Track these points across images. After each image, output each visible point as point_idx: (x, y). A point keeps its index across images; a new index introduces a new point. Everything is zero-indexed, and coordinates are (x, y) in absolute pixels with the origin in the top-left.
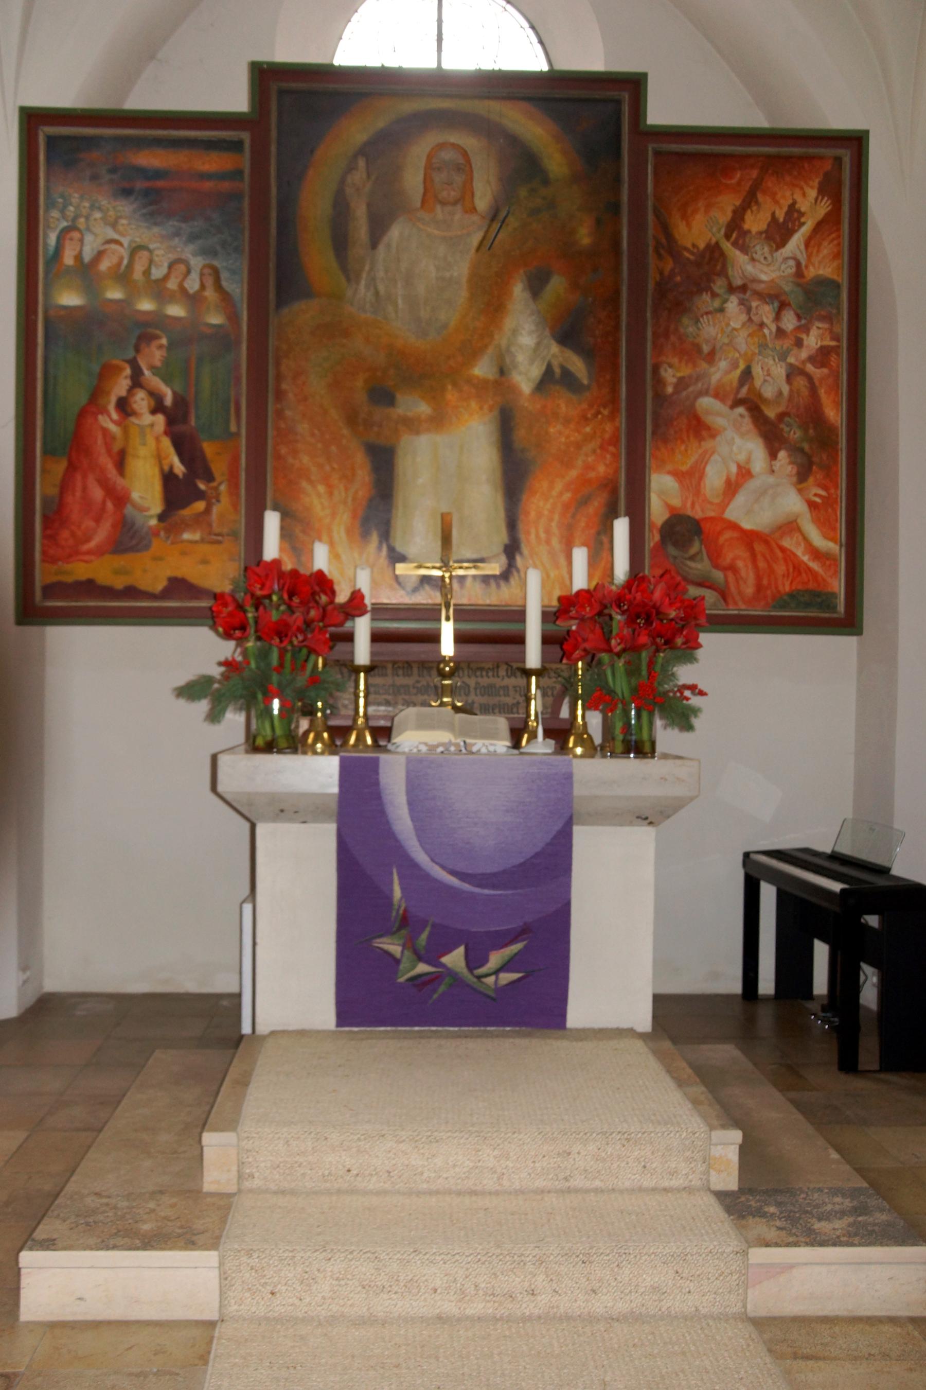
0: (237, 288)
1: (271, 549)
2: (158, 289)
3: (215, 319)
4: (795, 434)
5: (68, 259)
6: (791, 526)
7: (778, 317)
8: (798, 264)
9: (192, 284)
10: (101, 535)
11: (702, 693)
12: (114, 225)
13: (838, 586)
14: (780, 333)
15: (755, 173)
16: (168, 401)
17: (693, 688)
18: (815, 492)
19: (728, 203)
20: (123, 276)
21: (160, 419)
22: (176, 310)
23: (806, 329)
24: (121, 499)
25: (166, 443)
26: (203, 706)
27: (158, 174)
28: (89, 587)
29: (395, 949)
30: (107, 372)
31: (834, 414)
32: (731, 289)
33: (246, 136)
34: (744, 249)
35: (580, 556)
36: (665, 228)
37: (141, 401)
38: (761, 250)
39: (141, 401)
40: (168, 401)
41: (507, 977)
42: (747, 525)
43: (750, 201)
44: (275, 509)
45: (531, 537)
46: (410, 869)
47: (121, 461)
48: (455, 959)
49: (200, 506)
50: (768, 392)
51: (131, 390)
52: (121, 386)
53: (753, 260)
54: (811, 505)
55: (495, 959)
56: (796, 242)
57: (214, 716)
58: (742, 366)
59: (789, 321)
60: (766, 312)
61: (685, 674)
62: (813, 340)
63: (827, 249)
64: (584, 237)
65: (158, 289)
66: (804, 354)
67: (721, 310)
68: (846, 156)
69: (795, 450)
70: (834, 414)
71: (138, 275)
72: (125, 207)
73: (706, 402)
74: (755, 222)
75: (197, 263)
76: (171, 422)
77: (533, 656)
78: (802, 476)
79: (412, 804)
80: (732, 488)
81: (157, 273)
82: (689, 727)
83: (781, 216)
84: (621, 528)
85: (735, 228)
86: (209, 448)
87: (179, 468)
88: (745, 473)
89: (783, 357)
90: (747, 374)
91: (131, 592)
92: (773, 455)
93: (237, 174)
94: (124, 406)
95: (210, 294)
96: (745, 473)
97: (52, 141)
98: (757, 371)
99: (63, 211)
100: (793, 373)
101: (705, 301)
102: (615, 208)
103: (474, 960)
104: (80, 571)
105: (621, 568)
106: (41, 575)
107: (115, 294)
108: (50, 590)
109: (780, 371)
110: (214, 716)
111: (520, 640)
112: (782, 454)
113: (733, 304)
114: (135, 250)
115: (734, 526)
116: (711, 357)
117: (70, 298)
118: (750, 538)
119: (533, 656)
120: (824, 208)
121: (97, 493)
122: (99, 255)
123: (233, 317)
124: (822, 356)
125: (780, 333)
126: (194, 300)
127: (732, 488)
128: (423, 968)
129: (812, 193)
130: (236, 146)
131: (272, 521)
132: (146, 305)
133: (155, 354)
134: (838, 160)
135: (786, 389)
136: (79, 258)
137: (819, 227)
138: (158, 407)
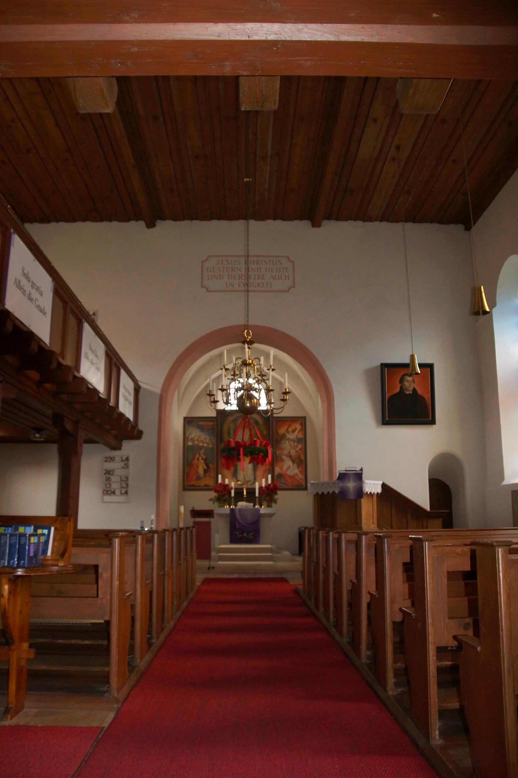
0: (215, 442)
1: (220, 481)
2: (202, 442)
3: (211, 446)
4: (297, 461)
5: (190, 438)
6: (296, 475)
7: (294, 443)
8: (297, 436)
9: (208, 441)
10: (195, 478)
11: (278, 499)
12: (196, 433)
13: (304, 483)
14: (294, 446)
15: (289, 423)
16: (204, 458)
17: (277, 498)
18: (300, 469)
19: (286, 427)
20: (198, 440)
21: (203, 461)
22: (205, 445)
23: (298, 445)
24: (197, 472)
25: (204, 465)
26: (212, 502)
27: (202, 425)
28: (193, 485)
29: (237, 533)
30: (195, 454)
31: (303, 457)
32: (287, 439)
33: (215, 420)
34: (288, 434)
35: (264, 480)
36: (277, 431)
37: (200, 458)
38: (291, 434)
39: (200, 458)
40: (204, 458)
41: (252, 537)
42: (289, 474)
43: (289, 426)
44: (220, 474)
45: (258, 477)
46: (239, 523)
47: (197, 468)
48: (245, 534)
49: (208, 474)
50: (293, 455)
51: (199, 457)
52: (197, 456)
53: (290, 435)
54: (300, 472)
55: (250, 535)
56: (296, 433)
57: (214, 503)
58: (289, 451)
59: (296, 444)
60: (292, 443)
61: (276, 497)
62: (300, 447)
63: (301, 433)
64: (265, 432)
65: (202, 442)
66: (298, 449)
67: (285, 443)
68: (303, 419)
69: (297, 463)
70: (303, 457)
71: (200, 440)
72: (198, 430)
73: (284, 457)
74: (290, 430)
75: (208, 438)
76: (204, 461)
77: (257, 495)
78: (298, 467)
79: (240, 514)
80: (287, 469)
81: (203, 439)
82: (276, 504)
83: (294, 428)
84: (270, 476)
85: (287, 430)
86: (210, 465)
87: (206, 468)
88: (289, 467)
89: (295, 449)
90: (289, 452)
91: (199, 486)
92: (293, 464)
93: (214, 425)
94: (198, 459)
95: (210, 442)
96: (289, 467)
97: (188, 421)
98: (291, 451)
99: (189, 431)
100: (296, 452)
101: (283, 442)
102: (269, 428)
103: (248, 534)
104: (192, 483)
105: (270, 482)
106: (186, 484)
107: (196, 443)
108: (188, 486)
109: (294, 451)
110: (214, 503)
111: (255, 493)
112: (295, 464)
113: (287, 442)
114: (199, 436)
115: (288, 475)
116: (284, 450)
117: (190, 443)
118: (290, 477)
119: (257, 495)
120: (300, 427)
121: (194, 472)
122: (194, 438)
123: (214, 446)
124: (301, 449)
125: (294, 446)
126: (208, 443)
127: (287, 469)
128: (241, 536)
129: (298, 425)
130: (214, 421)
131: (220, 476)
132: (201, 444)
133: (202, 451)
134: (302, 420)
135: (295, 454)
136: (191, 438)
137: (300, 430)
138: (203, 459)
